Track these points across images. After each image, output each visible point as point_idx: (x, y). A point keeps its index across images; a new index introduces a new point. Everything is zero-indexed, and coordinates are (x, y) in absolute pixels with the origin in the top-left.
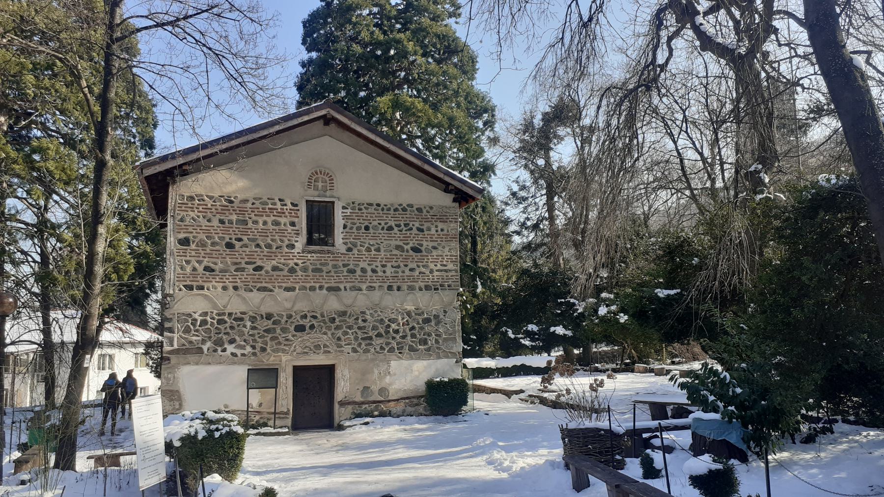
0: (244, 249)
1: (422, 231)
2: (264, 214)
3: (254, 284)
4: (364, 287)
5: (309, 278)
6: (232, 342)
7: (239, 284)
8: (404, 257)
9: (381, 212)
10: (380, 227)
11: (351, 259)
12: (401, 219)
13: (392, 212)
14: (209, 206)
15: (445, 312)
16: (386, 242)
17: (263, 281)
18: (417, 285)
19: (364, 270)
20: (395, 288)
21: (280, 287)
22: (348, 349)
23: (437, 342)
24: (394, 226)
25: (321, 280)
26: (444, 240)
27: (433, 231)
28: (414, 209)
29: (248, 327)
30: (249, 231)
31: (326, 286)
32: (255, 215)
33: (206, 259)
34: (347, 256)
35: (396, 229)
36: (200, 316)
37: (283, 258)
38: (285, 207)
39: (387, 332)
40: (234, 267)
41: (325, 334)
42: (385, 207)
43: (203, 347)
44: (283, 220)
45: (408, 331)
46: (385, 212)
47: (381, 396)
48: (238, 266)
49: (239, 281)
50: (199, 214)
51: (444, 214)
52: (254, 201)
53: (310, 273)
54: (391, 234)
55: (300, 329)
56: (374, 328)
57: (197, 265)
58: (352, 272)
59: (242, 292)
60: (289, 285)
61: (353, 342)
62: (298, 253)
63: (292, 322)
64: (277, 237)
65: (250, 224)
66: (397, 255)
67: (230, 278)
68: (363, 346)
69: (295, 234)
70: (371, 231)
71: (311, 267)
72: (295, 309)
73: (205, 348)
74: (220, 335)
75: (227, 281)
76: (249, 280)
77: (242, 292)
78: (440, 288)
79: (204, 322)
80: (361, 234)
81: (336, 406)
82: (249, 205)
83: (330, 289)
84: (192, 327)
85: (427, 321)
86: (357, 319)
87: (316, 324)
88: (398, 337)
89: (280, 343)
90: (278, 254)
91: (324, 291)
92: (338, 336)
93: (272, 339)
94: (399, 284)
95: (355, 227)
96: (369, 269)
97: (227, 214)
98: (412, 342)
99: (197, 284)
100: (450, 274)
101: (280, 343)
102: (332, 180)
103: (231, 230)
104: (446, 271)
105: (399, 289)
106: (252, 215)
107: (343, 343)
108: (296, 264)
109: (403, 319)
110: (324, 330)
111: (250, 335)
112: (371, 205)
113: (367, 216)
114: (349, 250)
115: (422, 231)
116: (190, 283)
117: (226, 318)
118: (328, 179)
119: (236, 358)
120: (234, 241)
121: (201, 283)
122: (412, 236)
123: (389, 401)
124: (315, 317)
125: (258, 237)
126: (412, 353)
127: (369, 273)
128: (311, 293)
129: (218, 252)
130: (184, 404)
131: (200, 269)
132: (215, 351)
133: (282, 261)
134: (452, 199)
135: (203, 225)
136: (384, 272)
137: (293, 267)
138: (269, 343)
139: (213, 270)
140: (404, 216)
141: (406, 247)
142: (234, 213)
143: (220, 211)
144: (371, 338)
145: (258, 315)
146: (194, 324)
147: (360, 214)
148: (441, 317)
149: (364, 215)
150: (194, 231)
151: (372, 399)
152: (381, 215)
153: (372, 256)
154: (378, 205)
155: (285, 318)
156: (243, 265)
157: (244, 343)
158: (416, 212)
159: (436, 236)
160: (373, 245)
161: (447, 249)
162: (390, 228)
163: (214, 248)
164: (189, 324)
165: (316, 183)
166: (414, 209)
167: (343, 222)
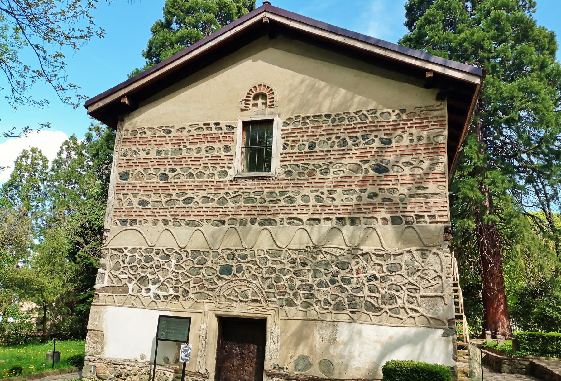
0: (176, 180)
2: (198, 141)
4: (304, 218)
5: (240, 210)
6: (156, 282)
7: (169, 218)
9: (331, 124)
10: (330, 143)
11: (290, 186)
12: (357, 130)
13: (346, 122)
14: (149, 139)
19: (306, 198)
21: (208, 221)
25: (253, 213)
30: (183, 160)
36: (130, 251)
37: (213, 188)
38: (219, 132)
42: (337, 118)
43: (129, 285)
44: (216, 146)
46: (337, 123)
47: (324, 372)
49: (168, 214)
50: (140, 147)
52: (190, 129)
53: (242, 203)
55: (227, 270)
58: (292, 200)
59: (170, 226)
62: (231, 181)
64: (209, 165)
65: (185, 154)
67: (161, 211)
70: (317, 149)
73: (130, 286)
75: (157, 214)
77: (170, 226)
80: (304, 154)
82: (185, 133)
84: (122, 263)
87: (244, 265)
96: (312, 196)
97: (164, 145)
98: (369, 296)
100: (432, 200)
102: (273, 93)
103: (166, 160)
108: (227, 193)
110: (253, 272)
113: (313, 131)
114: (289, 173)
116: (124, 217)
118: (267, 94)
120: (167, 172)
121: (134, 217)
124: (244, 257)
125: (190, 166)
126: (371, 313)
130: (106, 348)
131: (135, 202)
133: (213, 191)
134: (434, 96)
135: (142, 158)
139: (147, 203)
142: (170, 143)
143: (158, 142)
147: (304, 130)
150: (134, 165)
152: (331, 128)
153: (317, 181)
156: (175, 197)
164: (120, 260)
165: (255, 102)
167: (283, 141)
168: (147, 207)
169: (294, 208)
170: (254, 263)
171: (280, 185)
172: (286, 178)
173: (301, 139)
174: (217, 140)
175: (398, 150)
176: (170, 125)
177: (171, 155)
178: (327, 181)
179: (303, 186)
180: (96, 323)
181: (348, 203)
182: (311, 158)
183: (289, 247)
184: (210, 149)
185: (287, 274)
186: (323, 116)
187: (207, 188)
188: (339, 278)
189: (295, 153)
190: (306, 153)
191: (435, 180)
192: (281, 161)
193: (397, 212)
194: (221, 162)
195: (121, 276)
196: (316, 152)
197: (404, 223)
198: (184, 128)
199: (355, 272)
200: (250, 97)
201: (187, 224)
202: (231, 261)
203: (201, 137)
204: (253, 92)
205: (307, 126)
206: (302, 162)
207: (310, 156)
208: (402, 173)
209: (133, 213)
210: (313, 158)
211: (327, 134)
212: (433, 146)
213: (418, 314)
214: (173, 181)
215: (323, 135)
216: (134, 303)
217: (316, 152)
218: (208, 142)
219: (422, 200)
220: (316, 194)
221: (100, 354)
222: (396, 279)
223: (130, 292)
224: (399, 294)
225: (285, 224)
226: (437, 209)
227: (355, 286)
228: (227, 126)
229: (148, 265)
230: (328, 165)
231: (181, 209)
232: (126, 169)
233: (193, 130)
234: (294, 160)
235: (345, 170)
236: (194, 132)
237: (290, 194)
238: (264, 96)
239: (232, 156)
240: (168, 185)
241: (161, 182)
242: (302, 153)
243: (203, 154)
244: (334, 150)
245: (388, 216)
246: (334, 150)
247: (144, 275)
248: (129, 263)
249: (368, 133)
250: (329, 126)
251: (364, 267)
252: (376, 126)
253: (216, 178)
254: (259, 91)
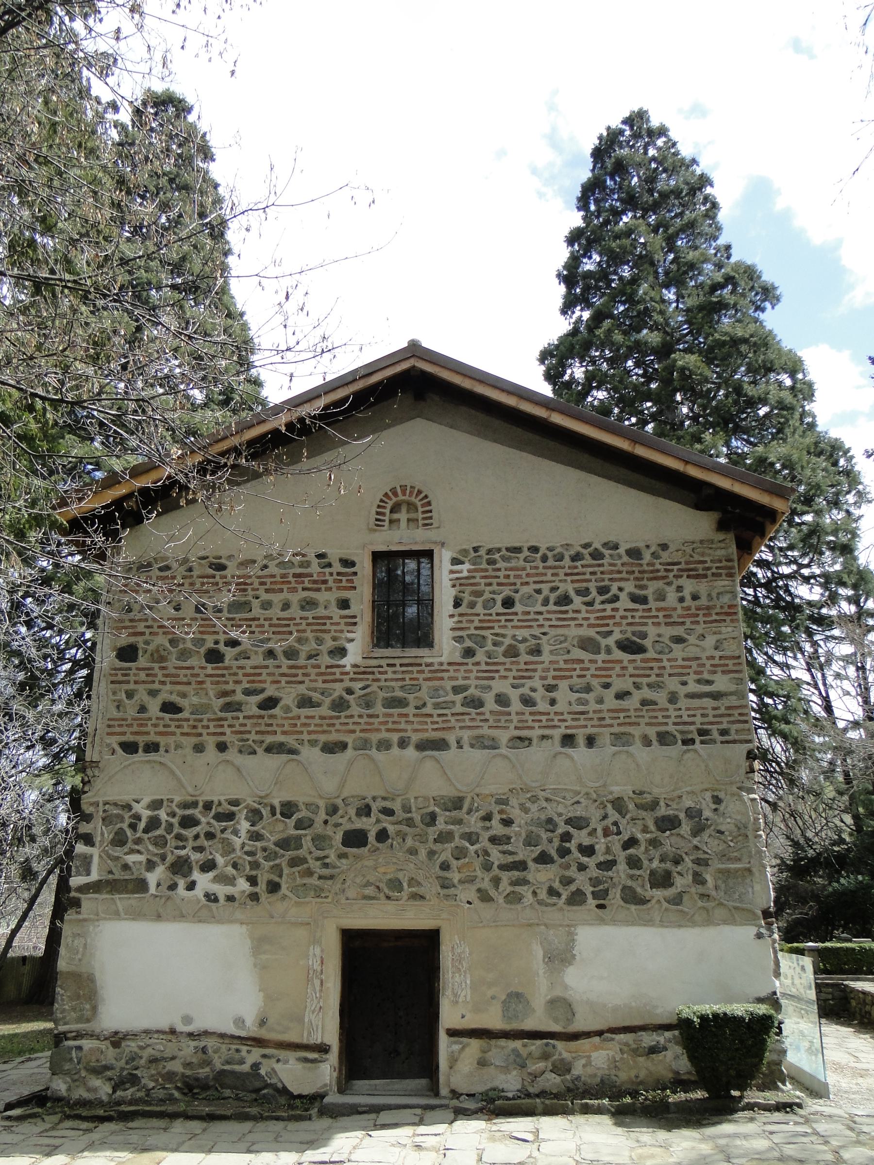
0: (242, 662)
1: (644, 600)
2: (285, 587)
3: (258, 737)
4: (504, 737)
5: (376, 721)
6: (208, 866)
7: (229, 738)
8: (600, 664)
9: (541, 565)
10: (540, 598)
11: (473, 675)
12: (588, 576)
13: (567, 561)
15: (717, 800)
16: (553, 632)
17: (279, 730)
18: (636, 732)
19: (502, 700)
20: (581, 740)
21: (313, 743)
22: (468, 893)
23: (699, 880)
24: (572, 594)
26: (701, 619)
27: (672, 597)
28: (622, 550)
29: (243, 833)
31: (415, 738)
32: (267, 591)
33: (168, 687)
34: (462, 668)
35: (578, 600)
37: (320, 679)
38: (327, 570)
39: (564, 852)
40: (222, 701)
41: (413, 852)
42: (550, 554)
44: (322, 597)
45: (617, 848)
46: (551, 562)
47: (556, 1020)
48: (228, 699)
49: (228, 731)
51: (697, 557)
53: (379, 709)
54: (566, 612)
56: (530, 841)
57: (146, 698)
58: (476, 703)
59: (232, 754)
60: (334, 737)
61: (479, 873)
63: (337, 825)
64: (309, 635)
65: (257, 611)
66: (582, 661)
67: (211, 724)
68: (505, 886)
69: (347, 624)
70: (518, 608)
71: (382, 694)
72: (345, 794)
73: (152, 878)
74: (183, 853)
75: (204, 732)
76: (248, 728)
78: (698, 739)
79: (153, 823)
80: (494, 617)
81: (443, 1040)
83: (422, 746)
84: (129, 832)
85: (668, 824)
86: (488, 817)
87: (391, 829)
88: (591, 862)
89: (309, 873)
90: (310, 670)
91: (411, 752)
92: (443, 857)
93: (294, 862)
94: (590, 731)
95: (480, 600)
96: (514, 696)
98: (631, 877)
99: (146, 738)
101: (309, 873)
104: (716, 696)
105: (591, 741)
106: (261, 592)
107: (455, 877)
108: (350, 691)
109: (605, 817)
110: (409, 842)
111: (248, 853)
112: (517, 550)
113: (508, 577)
114: (469, 653)
115: (644, 600)
117: (196, 812)
118: (419, 504)
119: (213, 905)
120: (221, 647)
121: (153, 738)
122: (618, 615)
123: (575, 1036)
126: (633, 907)
127: (516, 705)
128: (380, 756)
129: (189, 672)
130: (102, 1009)
131: (154, 707)
132: (173, 887)
133: (320, 685)
134: (714, 526)
136: (553, 702)
137: (341, 698)
138: (286, 871)
140: (596, 569)
141: (603, 642)
144: (521, 866)
145: (266, 805)
146: (133, 827)
148: (707, 813)
149: (501, 574)
150: (147, 631)
151: (529, 1025)
152: (541, 570)
154: (534, 549)
155: (322, 815)
156: (239, 697)
157: (234, 872)
158: (626, 559)
159: (679, 611)
160: (525, 640)
161: (711, 641)
162: (564, 600)
163: (185, 664)
164: (125, 826)
165: (395, 516)
166: (622, 550)
167: (453, 592)
168: (180, 716)
169: (482, 718)
170: (410, 822)
171: (451, 674)
172: (465, 661)
173: (488, 588)
174: (323, 586)
175: (661, 614)
176: (223, 553)
177: (229, 612)
178: (539, 667)
179: (496, 675)
180: (80, 956)
181: (581, 708)
182: (509, 624)
183: (477, 790)
184: (308, 603)
185: (477, 841)
186: (526, 549)
187: (307, 679)
188: (572, 845)
189: (478, 615)
190: (498, 614)
191: (725, 668)
192: (453, 629)
193: (666, 724)
194: (334, 628)
195: (131, 859)
196: (516, 614)
197: (680, 742)
198: (254, 562)
199: (600, 832)
200: (384, 507)
201: (268, 750)
202: (364, 819)
203: (291, 579)
204: (390, 499)
205: (497, 566)
206: (492, 631)
207: (506, 620)
208: (670, 656)
209: (149, 728)
210: (512, 624)
211: (535, 582)
212: (718, 610)
213: (712, 904)
214: (236, 663)
215: (527, 583)
216: (161, 910)
217: (516, 614)
218: (304, 589)
219: (708, 702)
220: (521, 691)
221: (88, 1021)
222: (670, 842)
223: (152, 889)
224: (679, 868)
225: (466, 747)
226: (732, 719)
227: (602, 859)
228: (341, 560)
229: (189, 833)
230: (540, 639)
231: (255, 721)
232: (132, 640)
233: (272, 564)
234: (476, 628)
235: (570, 648)
236: (273, 569)
237: (472, 691)
238: (412, 507)
239: (355, 617)
240: (225, 672)
241: (209, 666)
242: (491, 615)
243: (295, 611)
244: (549, 612)
245: (652, 732)
246: (549, 612)
247: (183, 853)
248: (146, 831)
249: (606, 583)
250: (537, 568)
251: (616, 824)
252: (620, 572)
253: (326, 660)
254: (401, 497)
